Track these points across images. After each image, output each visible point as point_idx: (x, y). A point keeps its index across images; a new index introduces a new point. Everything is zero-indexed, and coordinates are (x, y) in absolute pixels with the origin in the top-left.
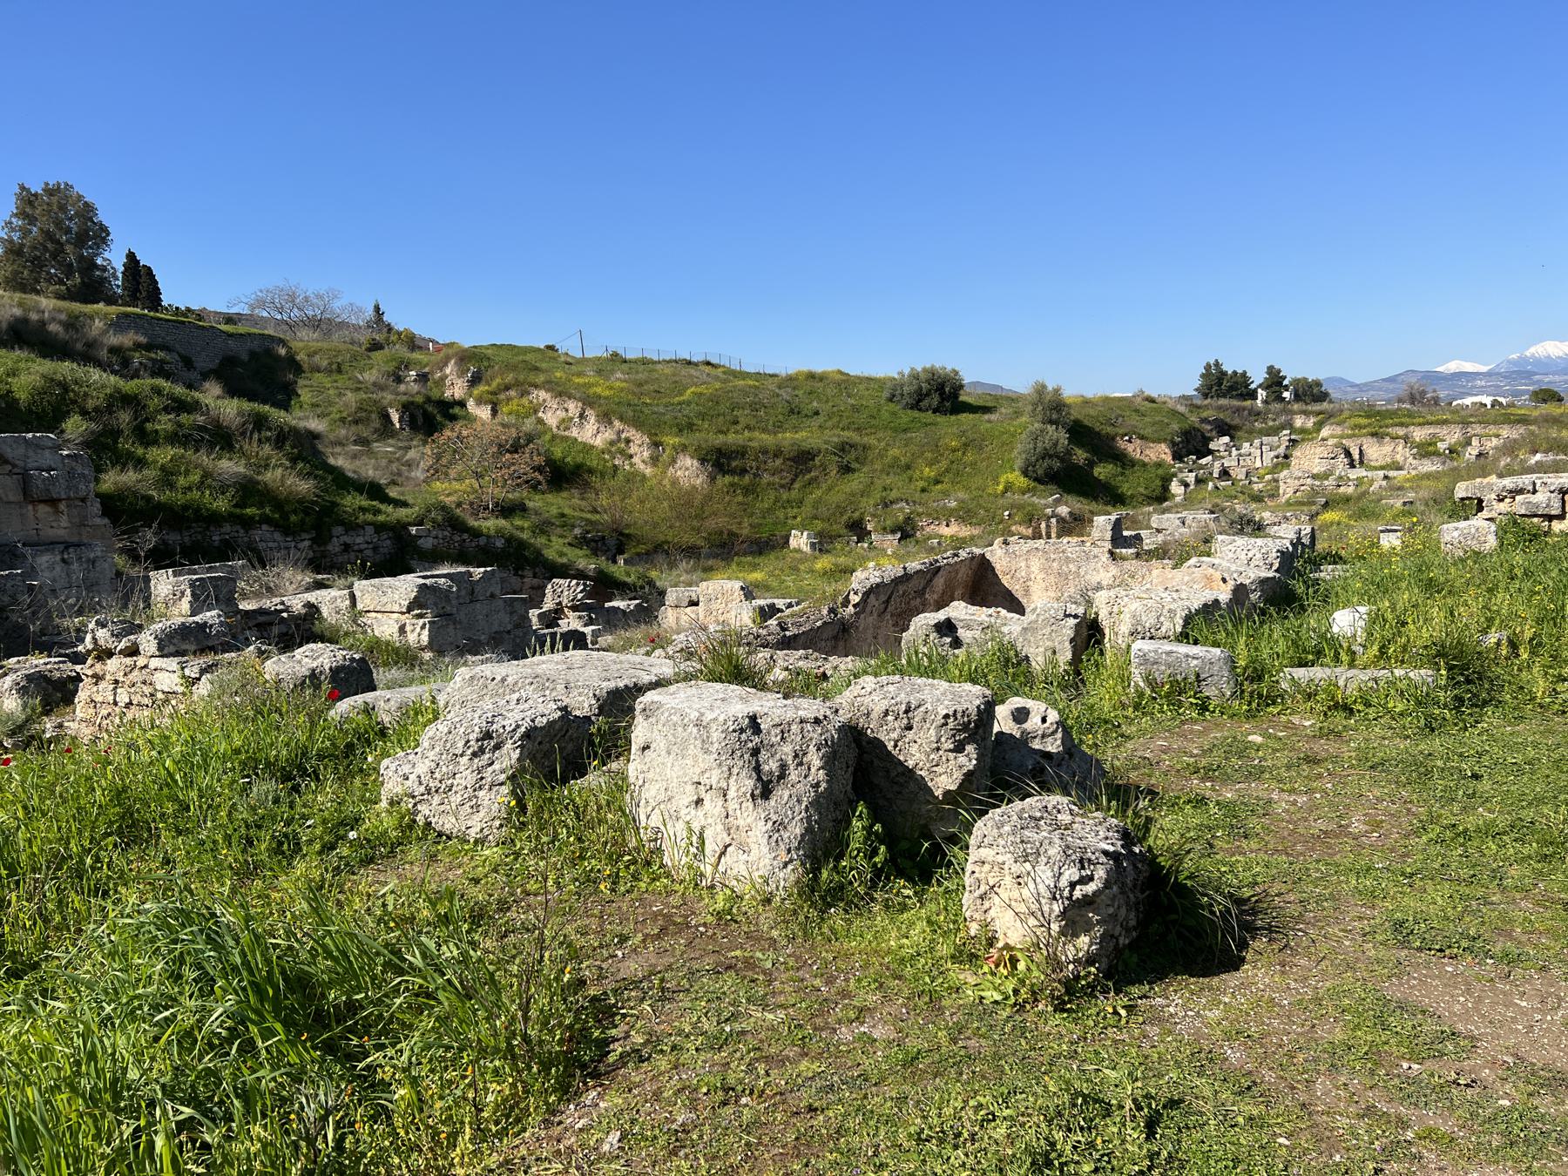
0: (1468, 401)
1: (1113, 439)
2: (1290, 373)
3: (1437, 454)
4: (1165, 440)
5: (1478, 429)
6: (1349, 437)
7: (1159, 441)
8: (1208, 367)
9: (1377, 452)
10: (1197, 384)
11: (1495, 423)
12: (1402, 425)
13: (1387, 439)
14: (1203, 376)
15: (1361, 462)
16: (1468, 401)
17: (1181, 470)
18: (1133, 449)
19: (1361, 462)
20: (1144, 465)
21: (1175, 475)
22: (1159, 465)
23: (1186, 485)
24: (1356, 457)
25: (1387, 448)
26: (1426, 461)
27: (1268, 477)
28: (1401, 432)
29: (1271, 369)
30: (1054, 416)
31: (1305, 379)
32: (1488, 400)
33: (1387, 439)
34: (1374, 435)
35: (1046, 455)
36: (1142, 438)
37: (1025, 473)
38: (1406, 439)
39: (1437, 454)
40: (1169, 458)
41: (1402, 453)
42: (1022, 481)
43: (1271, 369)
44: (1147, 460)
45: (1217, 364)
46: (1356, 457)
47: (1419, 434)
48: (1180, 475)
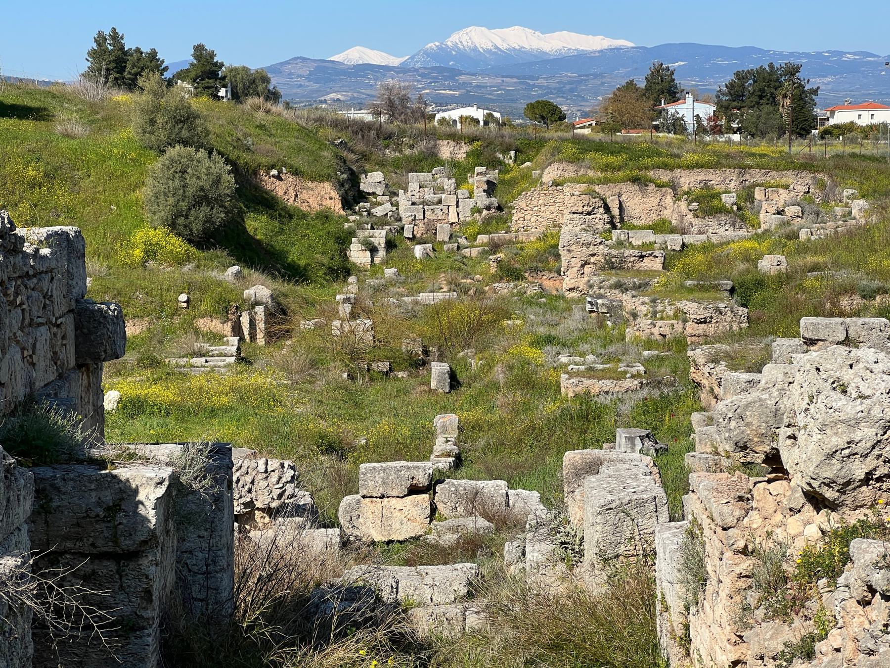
0: (455, 114)
1: (255, 173)
2: (229, 58)
3: (722, 210)
4: (328, 178)
5: (755, 176)
6: (605, 181)
7: (321, 178)
8: (100, 40)
9: (640, 205)
10: (85, 65)
11: (776, 168)
12: (665, 167)
13: (652, 187)
14: (93, 54)
15: (622, 220)
16: (455, 114)
17: (360, 226)
18: (282, 188)
19: (622, 220)
20: (304, 216)
21: (351, 234)
22: (325, 216)
23: (373, 250)
24: (616, 212)
25: (652, 200)
26: (711, 222)
27: (483, 238)
28: (664, 176)
29: (199, 51)
30: (185, 134)
31: (245, 70)
32: (479, 114)
33: (652, 187)
34: (635, 180)
35: (202, 199)
36: (296, 172)
37: (172, 225)
38: (674, 186)
39: (722, 210)
40: (336, 206)
41: (674, 210)
42: (177, 244)
43: (199, 51)
44: (304, 208)
45: (115, 36)
46: (616, 212)
47: (688, 180)
48: (362, 234)
